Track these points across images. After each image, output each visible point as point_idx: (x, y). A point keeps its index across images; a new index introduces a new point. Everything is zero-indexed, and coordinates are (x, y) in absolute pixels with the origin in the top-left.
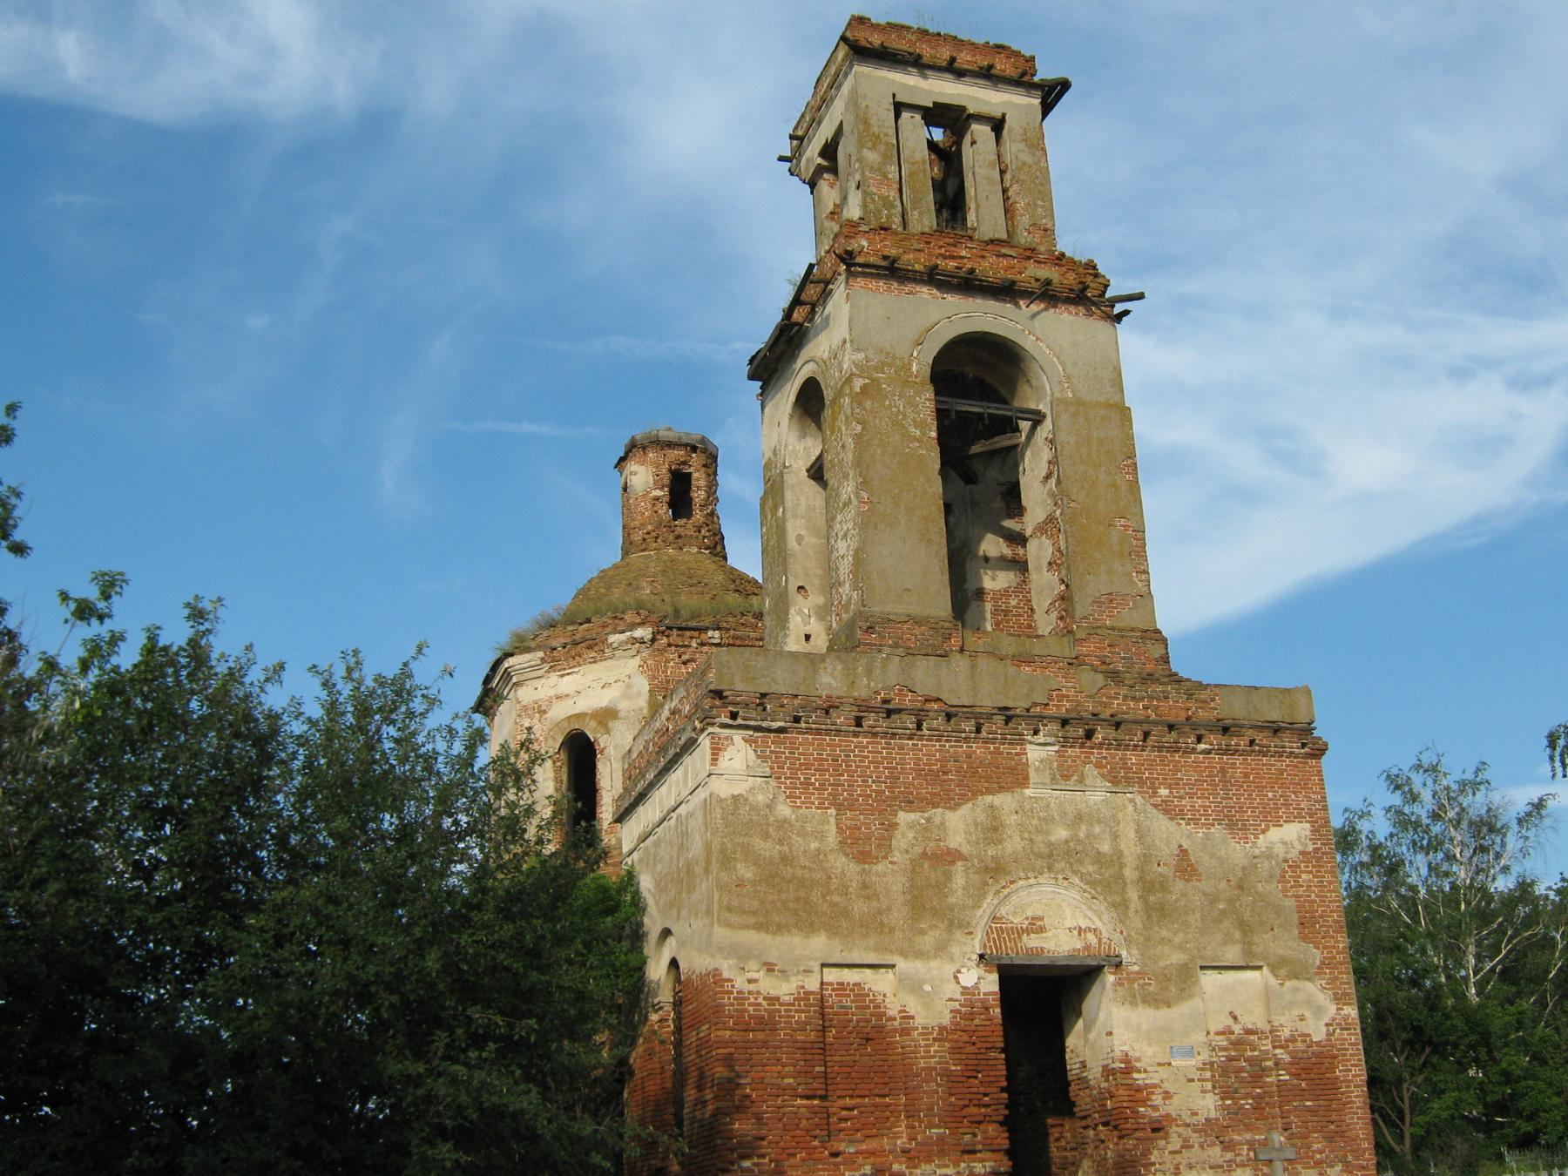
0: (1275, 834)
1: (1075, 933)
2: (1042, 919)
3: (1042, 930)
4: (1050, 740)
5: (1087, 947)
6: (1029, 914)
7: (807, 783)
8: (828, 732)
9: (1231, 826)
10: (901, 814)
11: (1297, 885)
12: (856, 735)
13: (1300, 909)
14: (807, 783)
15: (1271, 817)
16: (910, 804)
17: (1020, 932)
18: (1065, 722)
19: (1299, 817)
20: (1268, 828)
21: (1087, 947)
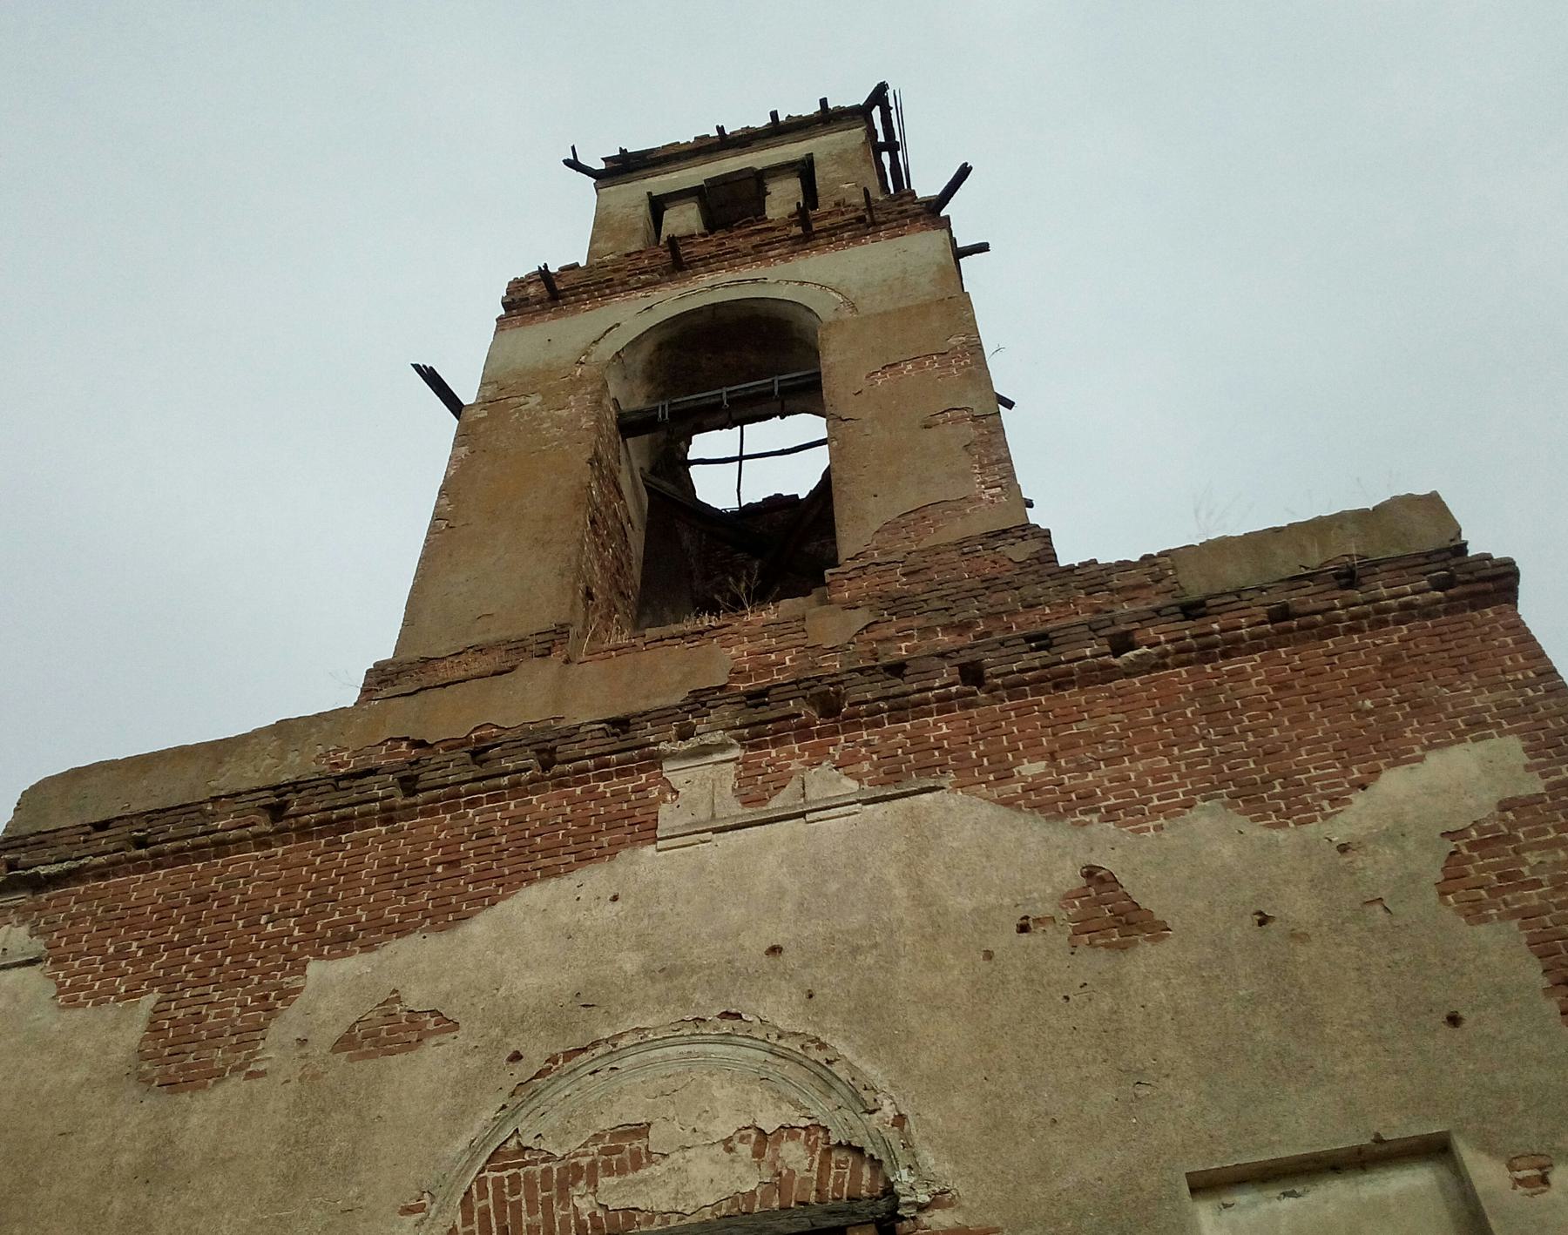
0: (1394, 782)
1: (745, 1150)
2: (641, 1130)
3: (637, 1161)
4: (718, 737)
5: (781, 1182)
6: (604, 1123)
7: (122, 953)
8: (199, 852)
9: (1249, 797)
10: (314, 968)
11: (1511, 879)
12: (262, 841)
13: (1543, 947)
14: (122, 953)
15: (1376, 747)
16: (342, 942)
17: (574, 1172)
18: (756, 698)
19: (1477, 727)
20: (1376, 772)
21: (781, 1182)
